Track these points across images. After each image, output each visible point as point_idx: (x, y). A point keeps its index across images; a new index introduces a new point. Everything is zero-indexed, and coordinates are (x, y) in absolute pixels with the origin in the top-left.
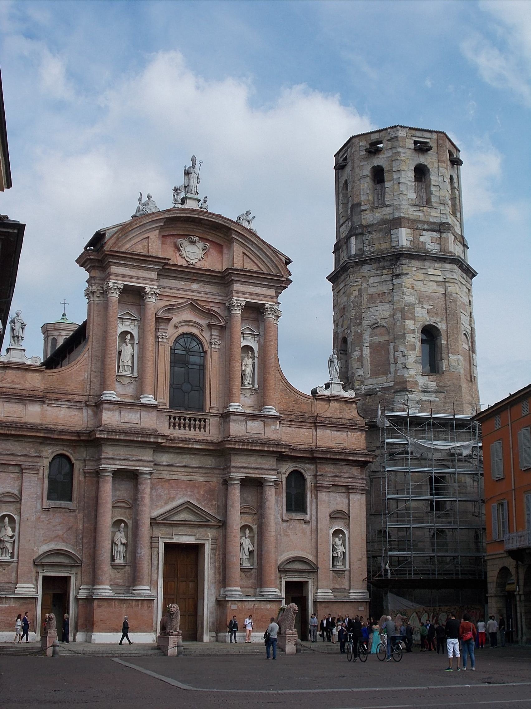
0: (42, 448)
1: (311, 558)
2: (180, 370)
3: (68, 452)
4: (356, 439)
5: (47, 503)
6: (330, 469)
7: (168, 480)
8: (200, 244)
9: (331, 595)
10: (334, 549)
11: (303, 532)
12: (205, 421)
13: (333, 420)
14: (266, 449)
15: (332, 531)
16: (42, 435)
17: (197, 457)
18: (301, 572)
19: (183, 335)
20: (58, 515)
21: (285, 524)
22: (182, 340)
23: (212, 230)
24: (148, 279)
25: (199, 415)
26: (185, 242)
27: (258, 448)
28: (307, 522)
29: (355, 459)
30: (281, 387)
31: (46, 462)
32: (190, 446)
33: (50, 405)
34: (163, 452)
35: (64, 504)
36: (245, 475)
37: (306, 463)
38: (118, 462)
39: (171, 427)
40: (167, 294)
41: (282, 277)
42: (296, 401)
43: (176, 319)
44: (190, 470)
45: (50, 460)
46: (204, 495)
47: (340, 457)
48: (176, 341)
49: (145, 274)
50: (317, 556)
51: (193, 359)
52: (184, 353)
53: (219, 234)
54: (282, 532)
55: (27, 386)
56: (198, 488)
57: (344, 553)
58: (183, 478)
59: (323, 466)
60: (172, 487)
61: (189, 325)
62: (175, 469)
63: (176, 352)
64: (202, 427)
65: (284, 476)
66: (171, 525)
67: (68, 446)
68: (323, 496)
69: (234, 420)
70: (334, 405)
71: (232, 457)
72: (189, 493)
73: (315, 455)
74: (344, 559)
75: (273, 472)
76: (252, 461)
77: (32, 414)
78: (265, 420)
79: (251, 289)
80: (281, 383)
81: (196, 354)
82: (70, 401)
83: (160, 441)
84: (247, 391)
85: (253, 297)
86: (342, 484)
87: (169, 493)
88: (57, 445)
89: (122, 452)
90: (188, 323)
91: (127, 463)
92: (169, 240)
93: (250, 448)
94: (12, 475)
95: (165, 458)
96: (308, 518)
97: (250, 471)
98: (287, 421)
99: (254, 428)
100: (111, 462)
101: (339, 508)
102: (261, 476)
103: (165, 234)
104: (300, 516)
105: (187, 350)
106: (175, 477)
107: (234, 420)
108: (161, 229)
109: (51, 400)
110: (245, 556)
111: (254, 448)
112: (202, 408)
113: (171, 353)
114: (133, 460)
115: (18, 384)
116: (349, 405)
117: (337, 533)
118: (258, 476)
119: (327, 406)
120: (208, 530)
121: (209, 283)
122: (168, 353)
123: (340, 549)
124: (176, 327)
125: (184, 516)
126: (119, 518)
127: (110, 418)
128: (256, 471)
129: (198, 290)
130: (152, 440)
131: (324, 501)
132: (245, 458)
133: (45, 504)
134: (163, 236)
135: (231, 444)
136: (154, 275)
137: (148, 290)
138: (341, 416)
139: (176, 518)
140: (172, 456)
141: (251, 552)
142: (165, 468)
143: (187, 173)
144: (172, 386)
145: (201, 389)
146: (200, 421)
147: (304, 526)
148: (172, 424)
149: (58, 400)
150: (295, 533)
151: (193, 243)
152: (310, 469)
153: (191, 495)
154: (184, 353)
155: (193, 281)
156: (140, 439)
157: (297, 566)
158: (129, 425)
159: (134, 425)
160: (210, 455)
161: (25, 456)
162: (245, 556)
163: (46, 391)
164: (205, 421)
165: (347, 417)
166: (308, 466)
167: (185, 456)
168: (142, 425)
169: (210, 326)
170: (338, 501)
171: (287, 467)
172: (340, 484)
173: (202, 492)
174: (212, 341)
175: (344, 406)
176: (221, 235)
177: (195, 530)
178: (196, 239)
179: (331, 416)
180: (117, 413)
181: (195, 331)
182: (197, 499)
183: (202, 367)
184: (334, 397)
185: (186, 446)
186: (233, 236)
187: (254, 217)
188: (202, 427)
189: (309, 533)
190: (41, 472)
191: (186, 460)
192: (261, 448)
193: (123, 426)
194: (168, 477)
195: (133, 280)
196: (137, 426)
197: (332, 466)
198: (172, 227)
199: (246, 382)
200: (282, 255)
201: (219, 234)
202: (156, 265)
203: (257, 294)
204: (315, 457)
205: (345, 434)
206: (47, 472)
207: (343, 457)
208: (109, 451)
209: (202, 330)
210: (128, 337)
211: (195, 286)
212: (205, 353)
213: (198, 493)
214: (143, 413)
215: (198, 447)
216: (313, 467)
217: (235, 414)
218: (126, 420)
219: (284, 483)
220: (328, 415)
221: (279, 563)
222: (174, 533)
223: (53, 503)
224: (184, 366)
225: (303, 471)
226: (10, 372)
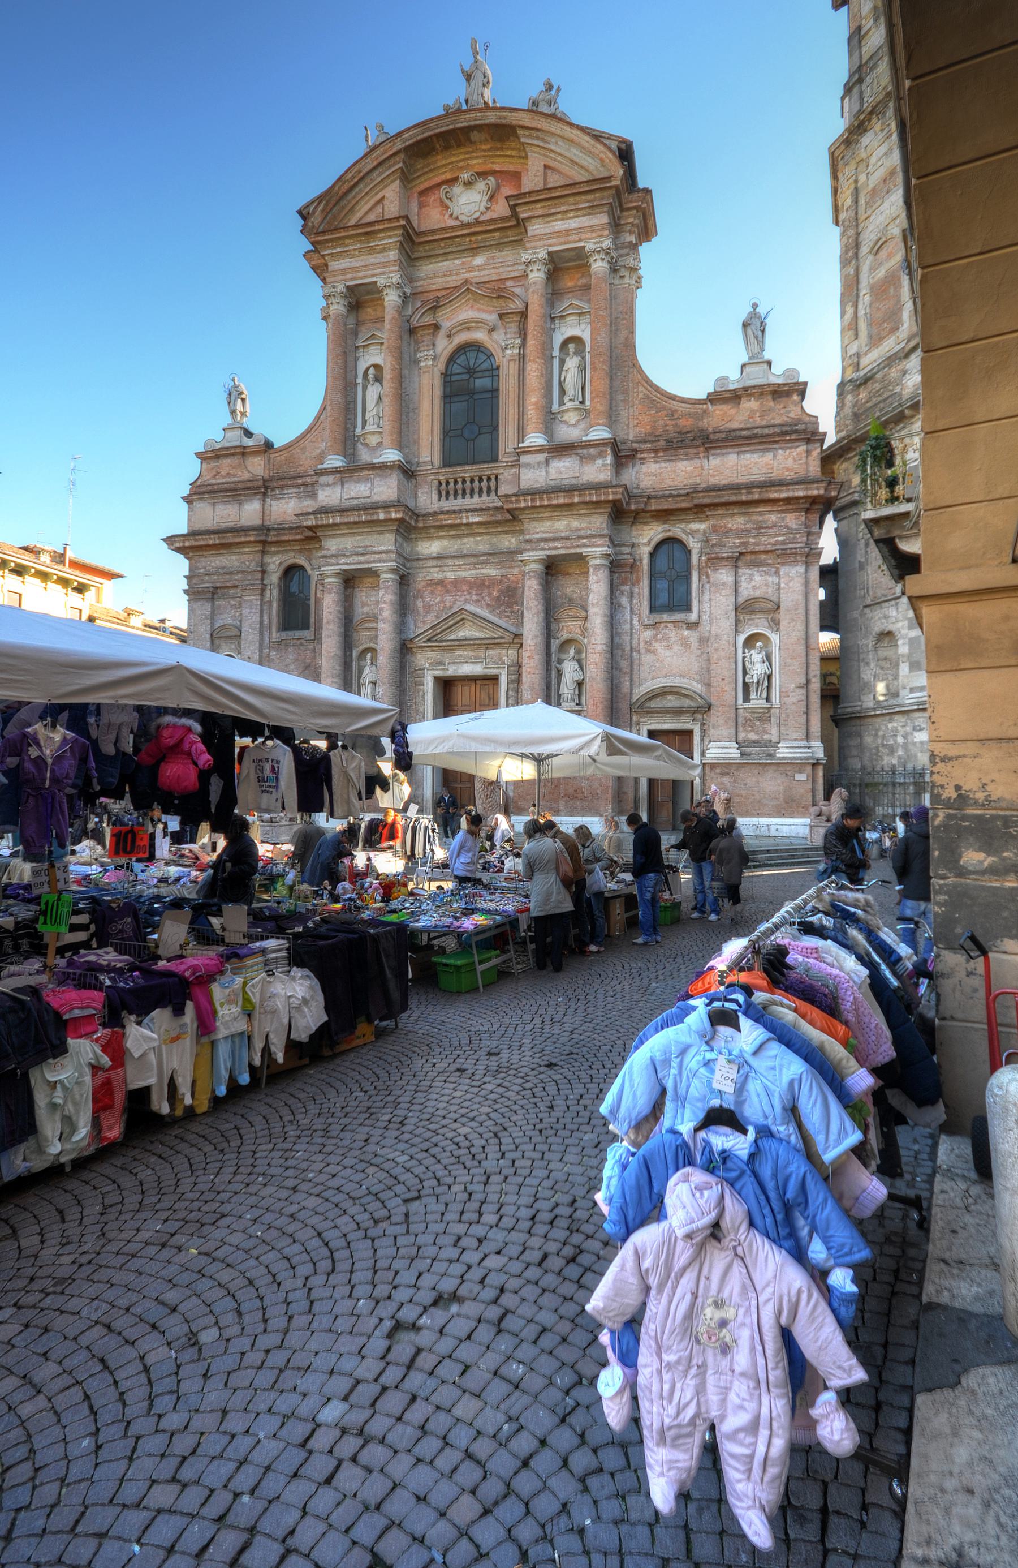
0: (268, 559)
1: (698, 687)
2: (459, 407)
3: (301, 561)
4: (795, 460)
5: (275, 635)
6: (737, 522)
7: (441, 582)
8: (481, 185)
9: (733, 752)
10: (745, 672)
11: (685, 643)
12: (496, 478)
13: (744, 433)
14: (576, 500)
15: (741, 638)
16: (252, 539)
17: (485, 537)
18: (678, 712)
19: (463, 349)
20: (291, 649)
21: (648, 634)
22: (463, 357)
23: (498, 149)
24: (383, 265)
25: (485, 469)
26: (457, 189)
27: (561, 501)
28: (693, 626)
29: (784, 495)
30: (641, 395)
31: (274, 578)
32: (465, 521)
33: (274, 498)
34: (431, 539)
35: (298, 634)
36: (548, 553)
37: (689, 522)
38: (343, 561)
39: (444, 498)
40: (434, 287)
41: (608, 178)
42: (673, 412)
43: (446, 324)
44: (473, 560)
45: (278, 574)
46: (498, 598)
47: (750, 497)
48: (452, 359)
49: (379, 258)
50: (708, 685)
51: (480, 383)
52: (465, 377)
53: (509, 153)
54: (642, 645)
55: (246, 476)
56: (489, 587)
57: (769, 677)
58: (463, 574)
59: (721, 523)
60: (448, 591)
61: (468, 329)
62: (449, 562)
63: (454, 378)
64: (493, 488)
65: (645, 551)
66: (443, 649)
67: (301, 551)
68: (724, 576)
69: (528, 465)
70: (751, 405)
71: (526, 525)
72: (474, 597)
73: (696, 501)
74: (769, 687)
75: (599, 541)
76: (561, 525)
77: (250, 512)
78: (585, 451)
79: (559, 225)
80: (641, 389)
81: (487, 374)
82: (298, 486)
83: (393, 516)
84: (571, 414)
85: (563, 240)
86: (762, 548)
87: (442, 601)
88: (287, 552)
89: (349, 543)
90: (466, 326)
91: (357, 558)
92: (432, 198)
93: (546, 503)
94: (232, 602)
95: (432, 547)
96: (693, 617)
97: (556, 544)
98: (649, 451)
99: (564, 469)
100: (333, 561)
101: (757, 594)
102: (579, 550)
103: (422, 187)
104: (678, 616)
105: (471, 372)
106: (450, 575)
107: (528, 465)
108: (406, 178)
109: (273, 489)
110: (566, 691)
111: (554, 502)
112: (495, 459)
113: (445, 384)
114: (363, 554)
115: (234, 476)
116: (784, 399)
117: (750, 641)
118: (573, 551)
119: (733, 411)
120: (504, 652)
121: (500, 245)
122: (438, 382)
123: (758, 670)
124: (449, 336)
125: (464, 632)
126: (368, 645)
127: (330, 495)
128: (568, 543)
129: (480, 266)
130: (382, 516)
131: (724, 584)
132: (548, 523)
133: (274, 635)
134: (422, 193)
135: (511, 502)
136: (393, 255)
137: (381, 281)
138: (764, 423)
139: (452, 637)
140: (445, 543)
141: (580, 684)
142: (434, 563)
143: (468, 77)
144: (446, 434)
145: (494, 428)
146: (489, 479)
147: (686, 633)
148: (444, 493)
149: (282, 488)
150: (668, 647)
151: (468, 184)
152: (698, 530)
153: (478, 601)
154: (465, 377)
155: (474, 251)
156: (364, 518)
157: (671, 701)
158: (356, 502)
159: (363, 501)
160: (506, 532)
161: (243, 572)
162: (566, 691)
163: (271, 479)
164: (496, 478)
165: (777, 421)
166: (694, 526)
167: (466, 540)
168: (376, 498)
169: (501, 316)
170: (755, 582)
171: (652, 533)
172: (757, 548)
173: (495, 594)
174: (502, 344)
175: (772, 404)
176: (514, 153)
177: (482, 653)
178: (465, 176)
179: (742, 426)
180: (338, 489)
181: (480, 336)
182: (488, 605)
183: (495, 391)
184: (745, 389)
185: (458, 521)
186: (523, 140)
187: (559, 89)
188: (493, 488)
189: (695, 644)
190: (268, 593)
191: (469, 544)
192: (567, 501)
193: (347, 504)
194: (440, 576)
195: (360, 274)
196: (369, 500)
197: (741, 520)
198: (431, 171)
199: (566, 399)
200: (610, 137)
201: (509, 153)
202: (390, 237)
203: (567, 232)
204: (701, 503)
205: (769, 456)
206: (275, 592)
207: (756, 496)
208: (332, 545)
209: (492, 330)
210: (371, 371)
211: (479, 260)
212: (498, 368)
213: (490, 595)
214: (377, 481)
215: (477, 519)
216: (703, 526)
217: (526, 452)
218: (353, 494)
219: (646, 561)
220: (735, 425)
221: (634, 699)
222: (447, 661)
223: (284, 635)
224: (467, 397)
225: (683, 536)
226: (226, 462)
